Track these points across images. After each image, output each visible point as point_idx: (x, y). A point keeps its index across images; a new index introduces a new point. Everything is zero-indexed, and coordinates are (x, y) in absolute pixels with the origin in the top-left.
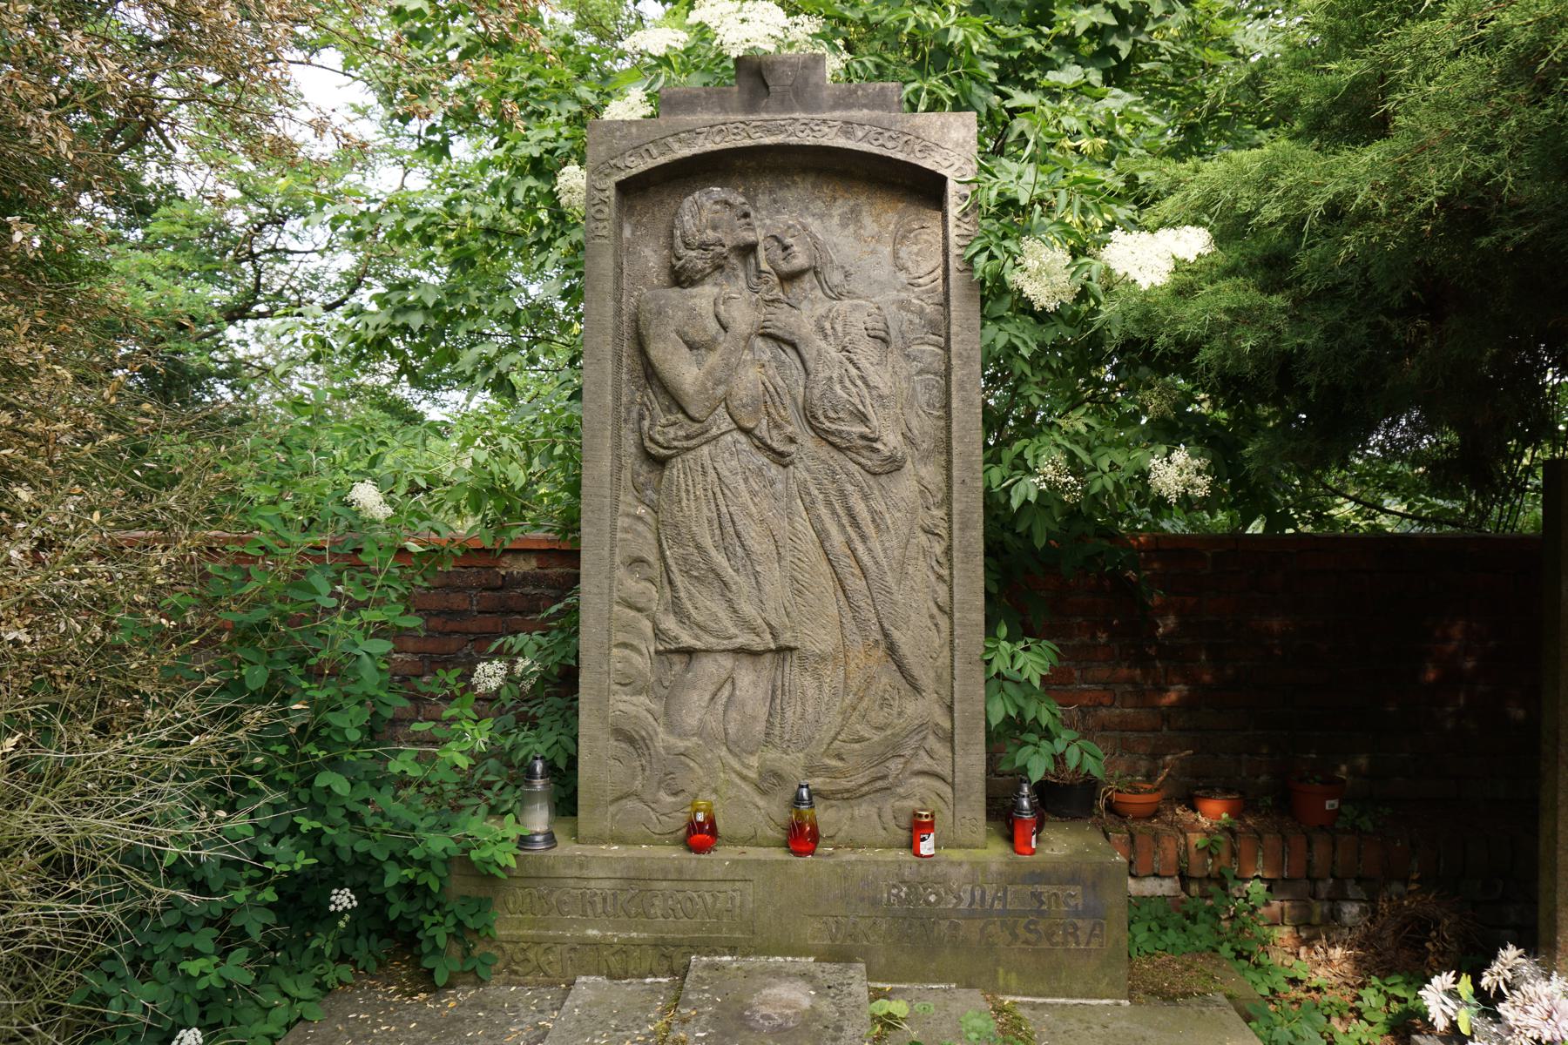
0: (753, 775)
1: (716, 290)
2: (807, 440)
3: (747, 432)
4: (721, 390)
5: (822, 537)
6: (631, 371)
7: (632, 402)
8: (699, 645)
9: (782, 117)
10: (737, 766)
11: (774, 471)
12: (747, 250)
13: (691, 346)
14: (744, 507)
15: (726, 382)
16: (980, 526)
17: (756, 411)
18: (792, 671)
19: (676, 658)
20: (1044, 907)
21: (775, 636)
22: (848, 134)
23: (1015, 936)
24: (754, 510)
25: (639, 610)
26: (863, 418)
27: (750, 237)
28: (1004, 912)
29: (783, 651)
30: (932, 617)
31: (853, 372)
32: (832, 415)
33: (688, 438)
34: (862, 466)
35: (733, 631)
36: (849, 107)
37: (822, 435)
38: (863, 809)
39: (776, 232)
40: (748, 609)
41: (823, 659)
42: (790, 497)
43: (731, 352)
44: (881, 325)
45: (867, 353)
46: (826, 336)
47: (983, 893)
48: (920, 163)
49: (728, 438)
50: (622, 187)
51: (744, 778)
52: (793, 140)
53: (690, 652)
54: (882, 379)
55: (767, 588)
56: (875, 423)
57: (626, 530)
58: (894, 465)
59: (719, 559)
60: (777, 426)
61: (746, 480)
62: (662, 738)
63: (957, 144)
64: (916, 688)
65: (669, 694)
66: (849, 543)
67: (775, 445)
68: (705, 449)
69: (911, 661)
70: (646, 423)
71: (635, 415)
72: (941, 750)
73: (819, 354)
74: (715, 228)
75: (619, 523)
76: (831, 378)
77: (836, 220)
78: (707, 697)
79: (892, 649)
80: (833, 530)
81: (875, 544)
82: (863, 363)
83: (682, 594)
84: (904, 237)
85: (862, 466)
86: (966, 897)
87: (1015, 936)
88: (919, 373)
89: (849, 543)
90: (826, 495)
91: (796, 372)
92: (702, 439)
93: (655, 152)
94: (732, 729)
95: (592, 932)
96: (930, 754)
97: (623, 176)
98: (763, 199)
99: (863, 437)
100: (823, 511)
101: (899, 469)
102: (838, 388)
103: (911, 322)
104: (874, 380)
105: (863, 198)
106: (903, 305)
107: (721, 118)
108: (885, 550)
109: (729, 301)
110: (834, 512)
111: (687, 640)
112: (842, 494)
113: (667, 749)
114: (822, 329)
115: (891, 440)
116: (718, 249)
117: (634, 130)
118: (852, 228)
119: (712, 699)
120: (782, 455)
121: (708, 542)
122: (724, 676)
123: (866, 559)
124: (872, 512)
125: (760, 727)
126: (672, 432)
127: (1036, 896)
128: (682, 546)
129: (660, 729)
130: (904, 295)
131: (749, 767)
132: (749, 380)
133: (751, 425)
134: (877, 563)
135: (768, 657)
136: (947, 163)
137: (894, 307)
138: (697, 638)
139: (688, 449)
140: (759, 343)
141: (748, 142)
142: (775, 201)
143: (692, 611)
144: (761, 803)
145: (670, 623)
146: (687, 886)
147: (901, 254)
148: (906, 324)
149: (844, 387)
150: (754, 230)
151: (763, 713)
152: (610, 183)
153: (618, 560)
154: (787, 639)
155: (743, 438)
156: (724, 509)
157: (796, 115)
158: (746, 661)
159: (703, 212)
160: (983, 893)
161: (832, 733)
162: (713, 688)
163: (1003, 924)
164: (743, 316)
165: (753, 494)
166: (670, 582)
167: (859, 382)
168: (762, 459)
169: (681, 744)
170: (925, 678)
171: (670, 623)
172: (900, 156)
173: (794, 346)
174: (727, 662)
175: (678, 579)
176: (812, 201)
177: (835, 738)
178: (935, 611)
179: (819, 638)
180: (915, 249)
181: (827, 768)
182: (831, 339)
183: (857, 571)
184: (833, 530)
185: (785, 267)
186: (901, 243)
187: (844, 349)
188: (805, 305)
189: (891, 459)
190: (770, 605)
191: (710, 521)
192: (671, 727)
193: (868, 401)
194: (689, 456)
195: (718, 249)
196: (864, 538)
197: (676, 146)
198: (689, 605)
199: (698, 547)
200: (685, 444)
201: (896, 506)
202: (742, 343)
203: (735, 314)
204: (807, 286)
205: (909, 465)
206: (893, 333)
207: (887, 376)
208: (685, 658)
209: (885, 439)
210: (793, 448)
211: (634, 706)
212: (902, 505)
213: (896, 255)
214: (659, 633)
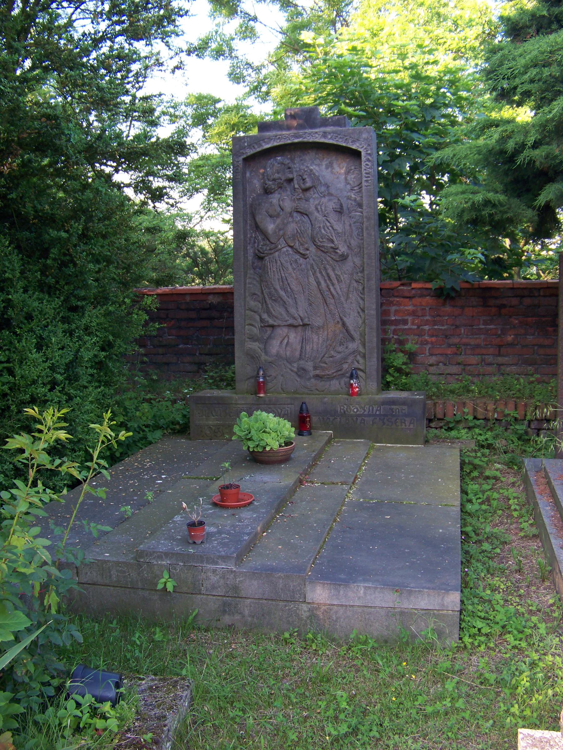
0: (295, 370)
1: (279, 196)
2: (313, 249)
3: (291, 247)
4: (281, 233)
5: (319, 283)
6: (251, 225)
7: (251, 237)
8: (275, 324)
10: (290, 367)
11: (302, 261)
12: (290, 181)
13: (271, 216)
14: (290, 274)
15: (283, 229)
17: (294, 239)
18: (309, 333)
19: (268, 329)
21: (302, 320)
23: (384, 423)
24: (294, 275)
25: (255, 312)
26: (332, 241)
27: (290, 176)
28: (380, 415)
29: (304, 325)
30: (358, 313)
31: (328, 224)
32: (321, 240)
33: (270, 249)
34: (332, 258)
35: (287, 318)
37: (318, 247)
38: (335, 382)
39: (301, 174)
40: (292, 311)
41: (319, 328)
42: (308, 270)
44: (339, 207)
45: (333, 218)
46: (318, 211)
49: (285, 249)
50: (245, 160)
51: (292, 371)
52: (305, 140)
53: (273, 326)
54: (339, 227)
55: (299, 303)
56: (336, 243)
57: (250, 283)
58: (344, 258)
59: (282, 293)
60: (302, 245)
61: (291, 264)
62: (263, 357)
63: (365, 139)
64: (353, 339)
65: (266, 342)
66: (328, 286)
67: (301, 252)
68: (277, 253)
69: (351, 328)
70: (256, 245)
71: (252, 241)
72: (361, 361)
74: (278, 173)
75: (247, 281)
77: (324, 167)
78: (279, 342)
79: (344, 324)
80: (322, 282)
81: (337, 287)
82: (332, 221)
83: (270, 306)
84: (349, 172)
85: (332, 258)
86: (367, 410)
87: (384, 423)
88: (354, 223)
89: (328, 286)
90: (320, 269)
91: (308, 225)
92: (275, 250)
93: (256, 147)
94: (288, 353)
96: (358, 362)
97: (245, 156)
98: (297, 160)
99: (332, 248)
100: (319, 275)
101: (346, 259)
102: (323, 231)
104: (336, 227)
105: (334, 158)
106: (349, 198)
109: (284, 200)
110: (322, 275)
111: (271, 322)
112: (325, 269)
113: (265, 361)
114: (317, 209)
115: (342, 249)
116: (279, 181)
118: (330, 169)
120: (304, 255)
121: (278, 287)
122: (285, 335)
124: (336, 275)
125: (297, 354)
126: (265, 248)
127: (392, 409)
128: (269, 289)
129: (263, 354)
130: (349, 194)
131: (294, 367)
132: (292, 228)
133: (292, 245)
135: (300, 328)
137: (345, 199)
138: (275, 321)
139: (271, 254)
140: (295, 214)
141: (289, 142)
142: (301, 160)
143: (273, 312)
144: (298, 380)
145: (265, 316)
146: (272, 406)
149: (325, 230)
150: (292, 173)
151: (299, 347)
152: (241, 159)
153: (247, 294)
154: (306, 321)
155: (290, 249)
156: (283, 275)
157: (306, 131)
158: (293, 330)
159: (273, 166)
162: (281, 339)
164: (288, 205)
165: (294, 269)
166: (266, 302)
168: (297, 257)
169: (270, 359)
170: (356, 335)
171: (265, 316)
172: (344, 145)
173: (307, 215)
174: (285, 330)
175: (269, 301)
176: (315, 159)
177: (324, 356)
178: (360, 310)
179: (318, 321)
180: (353, 176)
181: (321, 367)
183: (331, 296)
184: (322, 282)
185: (303, 186)
186: (348, 174)
187: (325, 216)
188: (311, 200)
190: (300, 309)
191: (278, 279)
192: (266, 353)
193: (334, 235)
194: (271, 256)
195: (279, 181)
196: (333, 285)
197: (263, 144)
198: (272, 310)
199: (274, 289)
200: (270, 252)
201: (344, 272)
203: (286, 204)
204: (312, 193)
205: (350, 257)
206: (345, 208)
207: (341, 225)
208: (271, 329)
209: (340, 248)
210: (308, 252)
211: (255, 346)
212: (347, 272)
213: (346, 179)
214: (262, 320)
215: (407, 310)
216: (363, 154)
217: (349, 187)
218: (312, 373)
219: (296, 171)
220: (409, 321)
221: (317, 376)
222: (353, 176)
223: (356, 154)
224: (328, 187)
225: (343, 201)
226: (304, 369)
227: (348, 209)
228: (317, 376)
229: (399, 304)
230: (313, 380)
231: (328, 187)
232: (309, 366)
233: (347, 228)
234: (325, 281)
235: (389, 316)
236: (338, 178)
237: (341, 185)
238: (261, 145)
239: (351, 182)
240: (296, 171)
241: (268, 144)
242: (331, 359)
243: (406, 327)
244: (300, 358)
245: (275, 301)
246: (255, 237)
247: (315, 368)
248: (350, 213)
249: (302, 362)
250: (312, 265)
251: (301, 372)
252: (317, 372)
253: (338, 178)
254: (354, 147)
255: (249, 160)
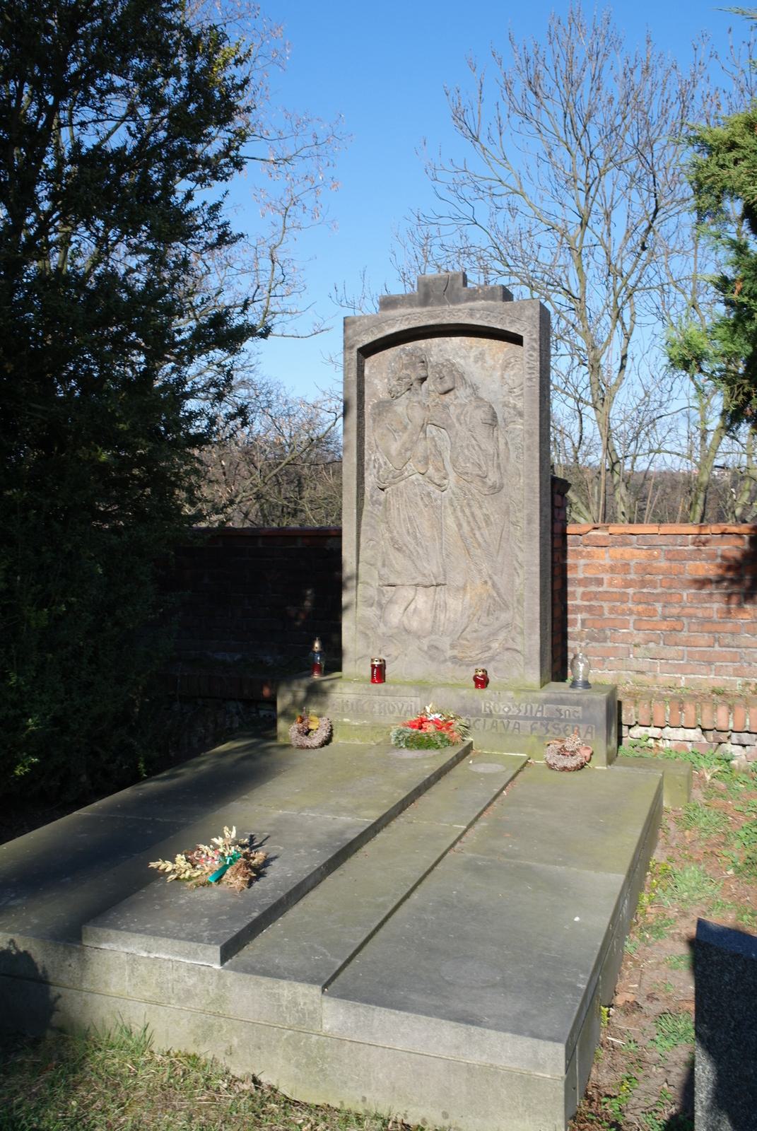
5: (460, 526)
9: (438, 309)
15: (411, 450)
16: (538, 521)
20: (563, 717)
21: (435, 578)
22: (471, 315)
26: (480, 467)
28: (542, 718)
31: (474, 442)
36: (474, 299)
42: (445, 507)
43: (413, 434)
44: (489, 417)
45: (481, 433)
46: (461, 424)
47: (532, 707)
48: (509, 330)
49: (413, 477)
56: (484, 469)
61: (422, 498)
63: (528, 318)
67: (436, 481)
68: (403, 483)
73: (457, 434)
76: (462, 446)
78: (403, 608)
80: (465, 524)
81: (486, 532)
84: (506, 367)
86: (523, 711)
87: (548, 731)
89: (472, 530)
90: (462, 507)
95: (345, 720)
96: (513, 640)
97: (360, 345)
100: (460, 514)
102: (466, 451)
103: (509, 413)
106: (506, 405)
107: (410, 310)
108: (490, 534)
110: (465, 515)
112: (469, 506)
117: (366, 321)
118: (480, 363)
119: (405, 609)
122: (411, 598)
123: (480, 540)
125: (428, 625)
127: (559, 711)
134: (485, 541)
136: (523, 328)
137: (501, 406)
140: (429, 428)
145: (385, 571)
147: (505, 376)
148: (506, 414)
151: (430, 616)
157: (446, 307)
160: (532, 707)
161: (463, 628)
162: (406, 604)
163: (541, 724)
165: (426, 506)
167: (477, 448)
168: (431, 488)
172: (499, 327)
180: (512, 373)
182: (464, 425)
183: (476, 545)
184: (465, 524)
186: (505, 370)
189: (493, 487)
191: (404, 520)
193: (481, 458)
198: (394, 562)
202: (419, 429)
206: (500, 419)
210: (446, 482)
215: (601, 565)
216: (525, 340)
217: (506, 388)
218: (449, 653)
219: (432, 367)
220: (605, 581)
221: (454, 659)
222: (512, 373)
223: (517, 340)
224: (478, 388)
225: (498, 409)
226: (436, 648)
227: (505, 420)
228: (454, 659)
229: (589, 556)
230: (449, 663)
231: (478, 388)
232: (445, 643)
233: (502, 446)
234: (469, 522)
235: (577, 573)
236: (491, 376)
237: (495, 386)
238: (382, 330)
239: (510, 382)
240: (432, 367)
241: (393, 327)
242: (475, 634)
243: (601, 589)
244: (432, 632)
245: (399, 550)
246: (375, 460)
247: (453, 647)
248: (507, 426)
249: (433, 637)
250: (451, 500)
251: (433, 652)
252: (455, 652)
253: (491, 376)
254: (512, 330)
255: (368, 351)
